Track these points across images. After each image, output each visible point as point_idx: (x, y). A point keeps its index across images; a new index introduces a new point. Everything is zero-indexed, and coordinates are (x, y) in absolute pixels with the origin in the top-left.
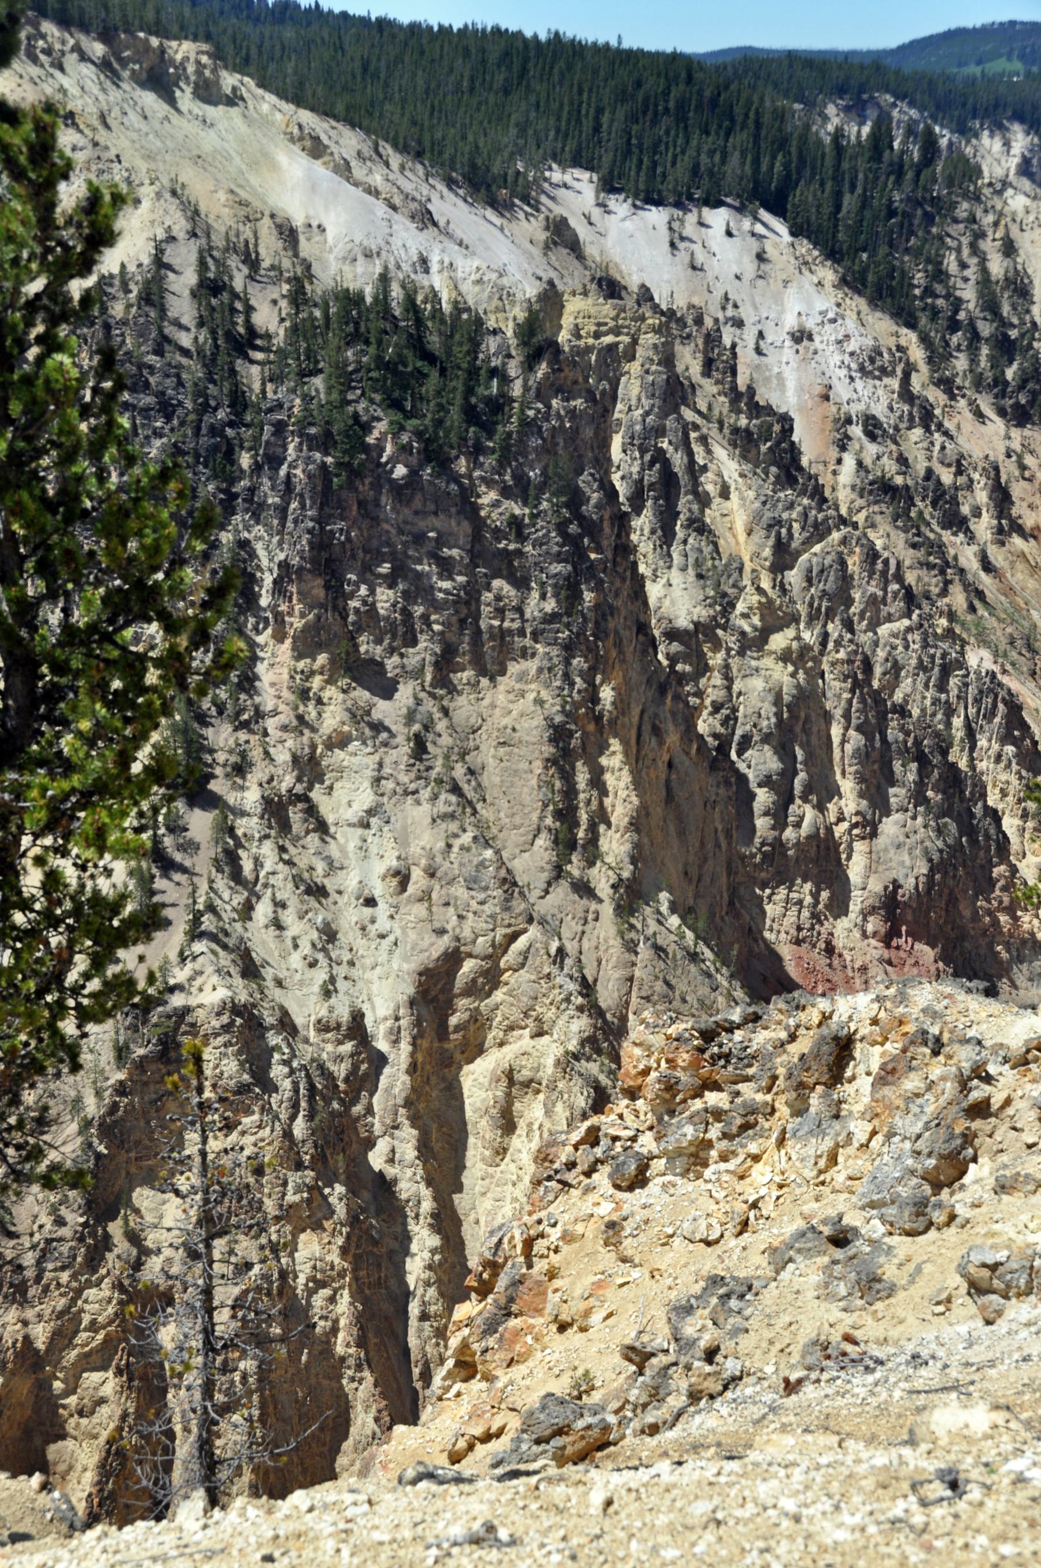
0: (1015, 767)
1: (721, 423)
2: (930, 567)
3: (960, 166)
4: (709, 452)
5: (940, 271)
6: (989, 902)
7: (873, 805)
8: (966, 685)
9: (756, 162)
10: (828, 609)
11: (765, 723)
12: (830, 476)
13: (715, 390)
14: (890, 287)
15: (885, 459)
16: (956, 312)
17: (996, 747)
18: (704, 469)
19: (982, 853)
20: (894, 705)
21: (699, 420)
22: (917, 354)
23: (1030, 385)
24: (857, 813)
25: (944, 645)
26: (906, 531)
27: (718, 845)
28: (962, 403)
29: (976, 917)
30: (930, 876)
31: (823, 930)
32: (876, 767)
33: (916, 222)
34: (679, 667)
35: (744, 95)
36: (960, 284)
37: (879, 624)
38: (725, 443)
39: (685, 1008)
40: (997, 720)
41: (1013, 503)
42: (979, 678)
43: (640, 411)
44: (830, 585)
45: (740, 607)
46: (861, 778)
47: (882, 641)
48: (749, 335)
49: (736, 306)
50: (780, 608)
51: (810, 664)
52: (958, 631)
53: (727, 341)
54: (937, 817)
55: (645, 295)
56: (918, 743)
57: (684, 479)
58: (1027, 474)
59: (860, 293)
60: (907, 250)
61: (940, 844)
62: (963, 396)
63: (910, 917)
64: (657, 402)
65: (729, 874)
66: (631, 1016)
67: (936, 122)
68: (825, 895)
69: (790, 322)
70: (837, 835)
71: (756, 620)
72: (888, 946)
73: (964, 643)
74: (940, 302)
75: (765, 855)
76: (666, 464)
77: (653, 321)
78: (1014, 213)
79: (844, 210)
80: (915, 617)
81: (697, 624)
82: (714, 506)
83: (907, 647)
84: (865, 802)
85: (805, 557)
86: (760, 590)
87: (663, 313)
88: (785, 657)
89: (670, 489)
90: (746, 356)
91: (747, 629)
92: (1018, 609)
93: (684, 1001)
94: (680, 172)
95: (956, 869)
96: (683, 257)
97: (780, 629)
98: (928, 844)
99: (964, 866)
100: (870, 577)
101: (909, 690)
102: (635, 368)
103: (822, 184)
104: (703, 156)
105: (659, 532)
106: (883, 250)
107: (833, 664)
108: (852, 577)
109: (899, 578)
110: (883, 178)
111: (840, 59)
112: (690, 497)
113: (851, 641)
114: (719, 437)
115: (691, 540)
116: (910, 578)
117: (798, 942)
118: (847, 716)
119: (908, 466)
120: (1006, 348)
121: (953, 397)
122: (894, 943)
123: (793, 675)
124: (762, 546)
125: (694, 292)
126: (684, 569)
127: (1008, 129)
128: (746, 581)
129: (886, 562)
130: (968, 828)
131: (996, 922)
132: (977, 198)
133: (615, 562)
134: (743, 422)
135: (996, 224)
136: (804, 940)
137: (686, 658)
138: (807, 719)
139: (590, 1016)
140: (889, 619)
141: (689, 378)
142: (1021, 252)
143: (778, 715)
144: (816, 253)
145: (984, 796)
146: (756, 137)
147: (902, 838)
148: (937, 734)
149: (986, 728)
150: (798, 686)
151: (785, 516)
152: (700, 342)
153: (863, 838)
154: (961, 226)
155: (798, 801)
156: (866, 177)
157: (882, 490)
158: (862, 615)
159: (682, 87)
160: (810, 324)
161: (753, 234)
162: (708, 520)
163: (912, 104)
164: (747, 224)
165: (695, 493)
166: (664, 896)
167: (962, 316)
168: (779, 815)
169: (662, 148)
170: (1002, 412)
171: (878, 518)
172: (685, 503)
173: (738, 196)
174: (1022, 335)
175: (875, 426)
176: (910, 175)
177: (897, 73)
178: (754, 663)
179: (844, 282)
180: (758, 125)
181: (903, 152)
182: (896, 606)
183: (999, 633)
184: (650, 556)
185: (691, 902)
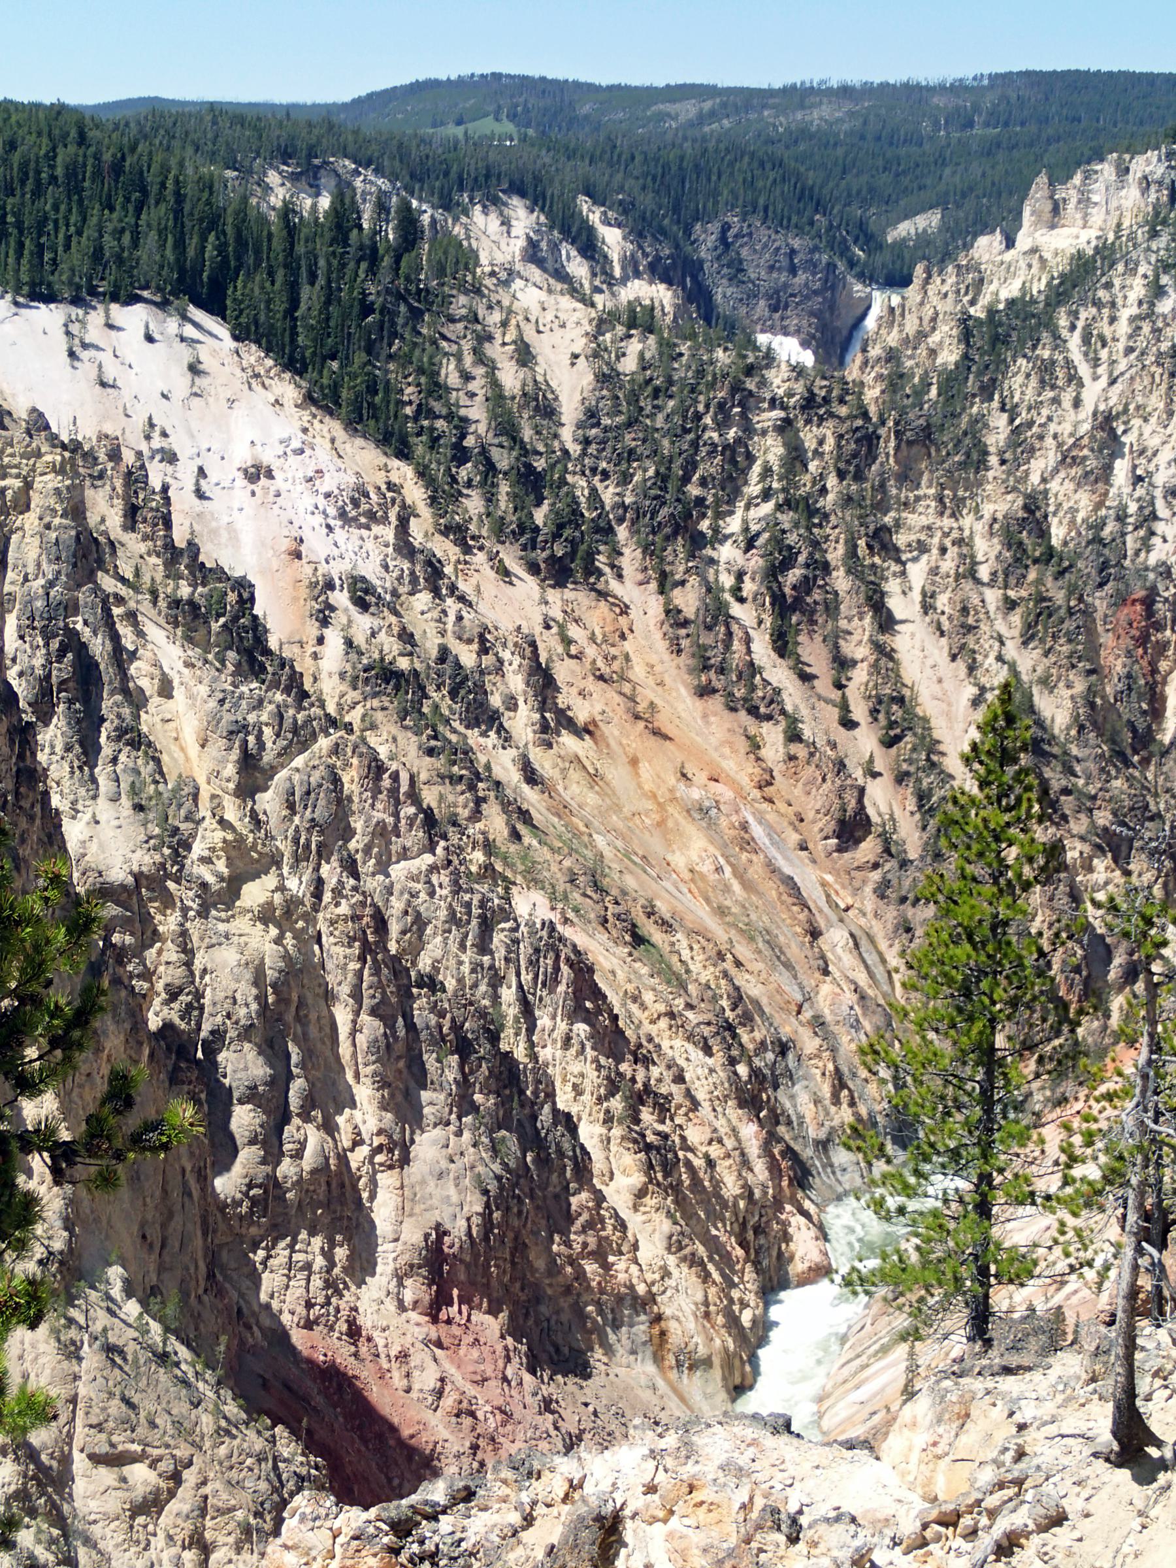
0: (590, 1053)
1: (154, 593)
2: (455, 780)
3: (452, 251)
4: (141, 634)
5: (437, 384)
6: (568, 1244)
7: (401, 1119)
8: (516, 942)
9: (180, 245)
10: (320, 846)
11: (243, 1011)
12: (309, 661)
13: (143, 548)
14: (371, 405)
15: (382, 636)
16: (463, 436)
17: (562, 1026)
18: (133, 655)
19: (554, 1177)
20: (420, 975)
21: (123, 591)
22: (415, 493)
23: (567, 533)
24: (380, 1132)
25: (483, 888)
26: (418, 733)
27: (187, 1193)
28: (480, 558)
29: (553, 1269)
30: (487, 1215)
31: (343, 1304)
32: (401, 1064)
33: (400, 321)
34: (116, 938)
35: (158, 158)
36: (464, 401)
37: (389, 863)
38: (162, 621)
39: (154, 1436)
40: (561, 988)
41: (558, 690)
42: (533, 933)
43: (41, 581)
44: (322, 810)
45: (198, 849)
46: (382, 1083)
47: (397, 888)
48: (185, 472)
49: (164, 434)
50: (254, 847)
51: (301, 924)
52: (499, 867)
53: (155, 482)
54: (492, 1131)
55: (38, 423)
56: (456, 1027)
57: (107, 671)
58: (573, 650)
59: (331, 414)
60: (390, 357)
61: (497, 1168)
62: (481, 548)
63: (462, 1277)
64: (65, 567)
65: (205, 1234)
66: (76, 1455)
67: (412, 194)
68: (341, 1253)
69: (242, 456)
70: (354, 1165)
71: (221, 866)
72: (435, 1320)
73: (509, 884)
74: (440, 424)
75: (254, 1201)
76: (81, 649)
77: (53, 457)
78: (526, 310)
79: (303, 307)
80: (439, 850)
81: (138, 877)
82: (151, 707)
83: (432, 894)
84: (389, 1116)
85: (282, 774)
86: (223, 823)
87: (64, 447)
88: (265, 916)
89: (87, 684)
90: (183, 504)
91: (210, 879)
92: (577, 835)
93: (153, 1425)
94: (76, 259)
95: (520, 1201)
96: (87, 370)
97: (257, 876)
98: (480, 1169)
99: (532, 1198)
100: (374, 798)
101: (438, 953)
102: (30, 521)
103: (271, 274)
104: (107, 237)
105: (78, 749)
106: (360, 357)
107: (332, 923)
108: (350, 799)
109: (414, 797)
110: (352, 265)
111: (281, 115)
112: (118, 698)
113: (355, 889)
114: (153, 613)
115: (122, 758)
116: (429, 797)
117: (309, 1325)
118: (356, 994)
119: (414, 645)
120: (531, 484)
121: (467, 550)
122: (443, 1316)
123: (278, 941)
124: (223, 761)
125: (105, 418)
126: (115, 799)
127: (506, 204)
128: (204, 810)
129: (395, 777)
130: (532, 1139)
131: (580, 1275)
132: (478, 291)
133: (17, 795)
134: (185, 591)
135: (504, 324)
136: (316, 1322)
137: (125, 924)
138: (301, 1004)
139: (17, 1459)
140: (404, 855)
141: (105, 533)
142: (539, 359)
143: (261, 998)
144: (269, 362)
145: (551, 1095)
146: (178, 213)
147: (444, 1164)
148: (482, 1014)
149: (547, 1000)
150: (286, 957)
151: (252, 718)
152: (119, 483)
153: (391, 1167)
154: (460, 326)
155: (296, 1121)
156: (329, 264)
157: (383, 677)
158: (367, 850)
159: (72, 149)
160: (268, 457)
161: (183, 339)
162: (144, 728)
163: (377, 171)
164: (172, 325)
165: (125, 691)
166: (115, 1273)
167: (470, 441)
168: (271, 1142)
169: (50, 227)
170: (533, 569)
171: (379, 716)
172: (110, 704)
173: (159, 289)
174: (552, 466)
175: (366, 591)
176: (387, 262)
177: (356, 132)
178: (222, 927)
179: (310, 399)
180: (179, 198)
181: (376, 233)
182: (414, 837)
183: (554, 868)
184: (66, 783)
185: (153, 1278)
